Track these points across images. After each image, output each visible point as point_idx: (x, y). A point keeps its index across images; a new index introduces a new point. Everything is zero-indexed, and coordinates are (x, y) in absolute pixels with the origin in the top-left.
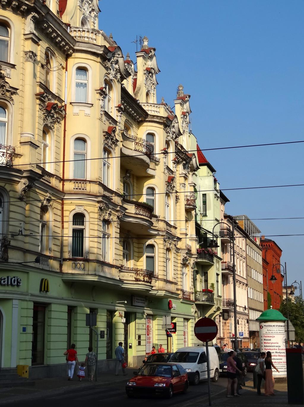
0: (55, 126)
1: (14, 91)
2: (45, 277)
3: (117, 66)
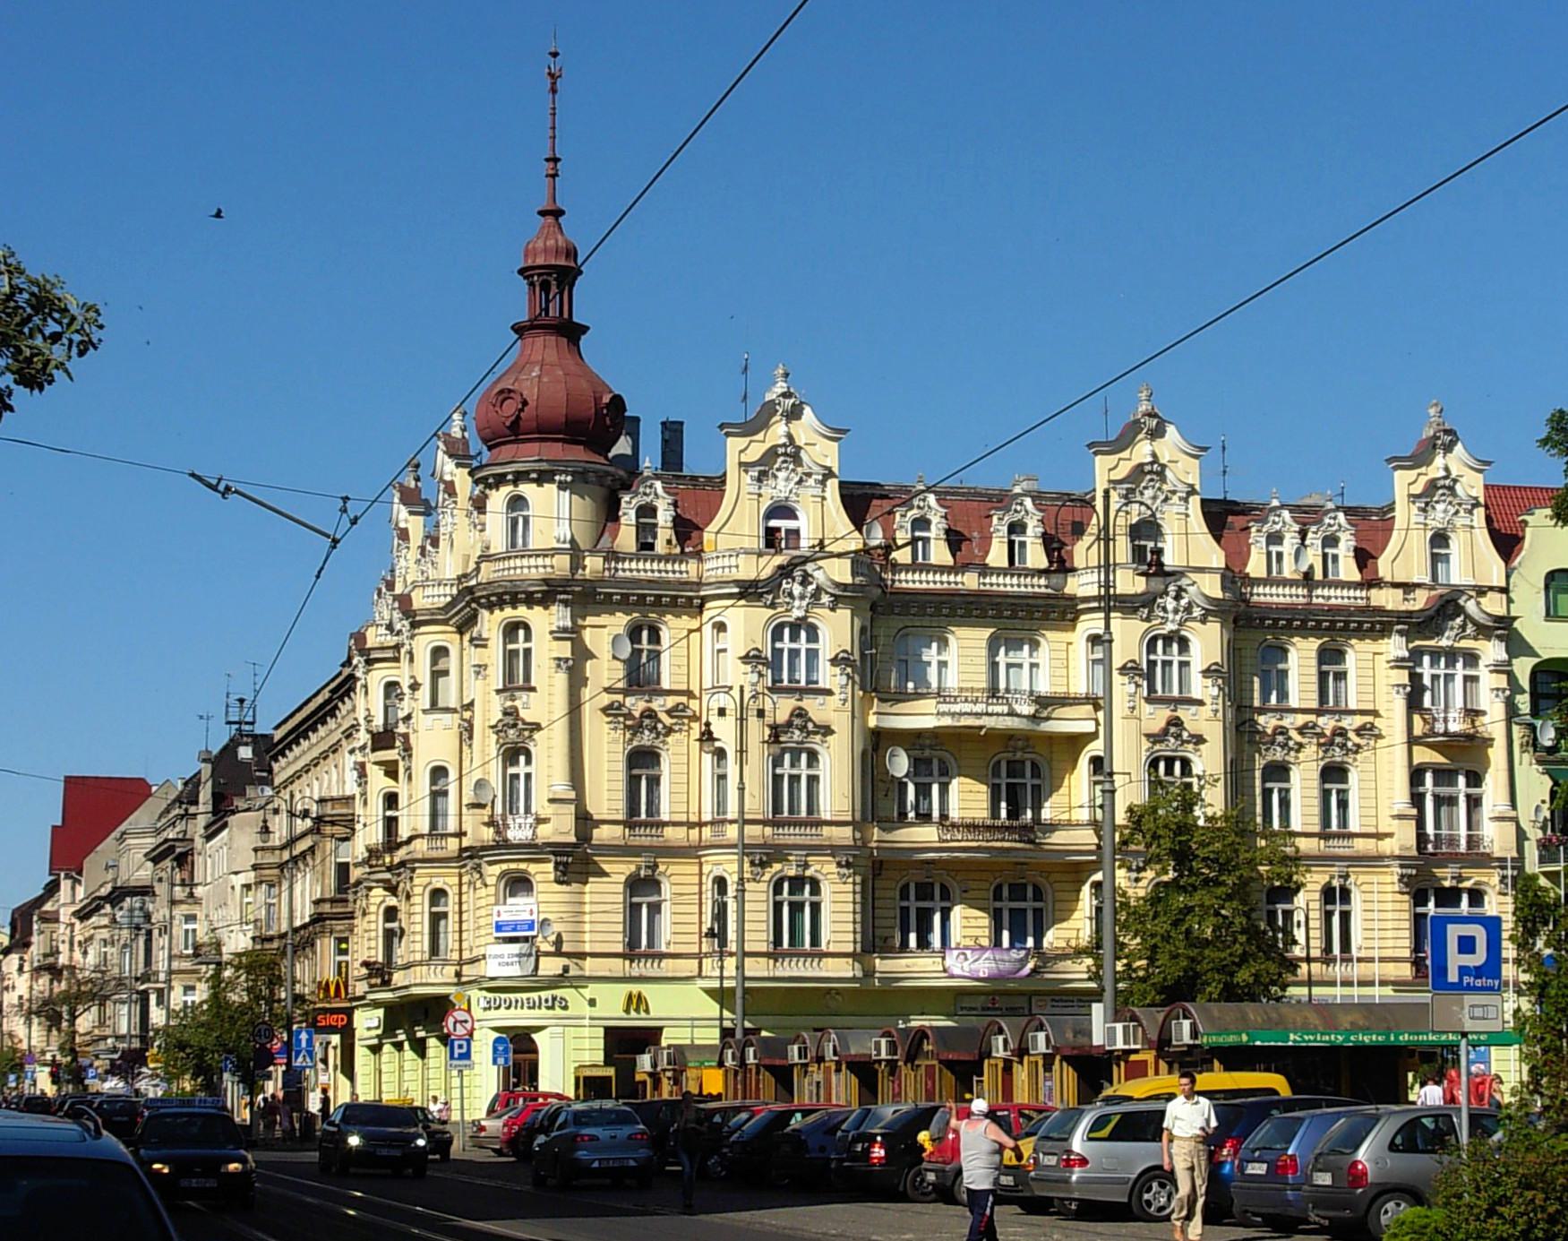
0: (669, 739)
1: (537, 727)
3: (811, 588)
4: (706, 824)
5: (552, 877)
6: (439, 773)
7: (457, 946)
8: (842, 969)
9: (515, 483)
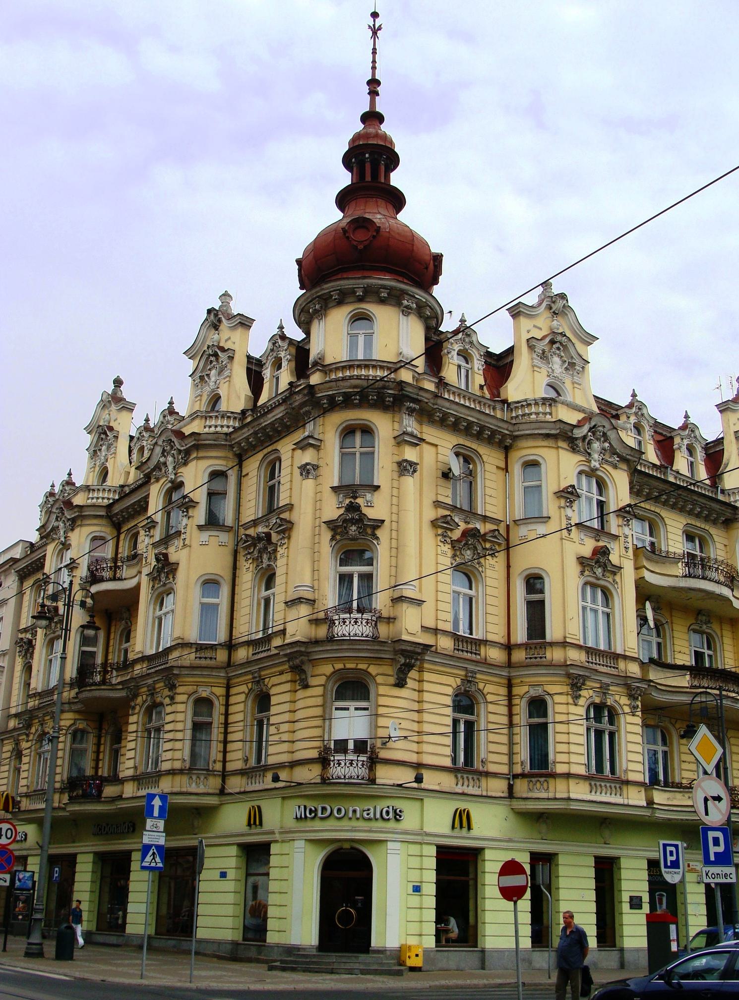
2: (462, 805)
4: (519, 646)
5: (392, 680)
6: (210, 584)
7: (220, 757)
8: (636, 798)
9: (361, 300)
